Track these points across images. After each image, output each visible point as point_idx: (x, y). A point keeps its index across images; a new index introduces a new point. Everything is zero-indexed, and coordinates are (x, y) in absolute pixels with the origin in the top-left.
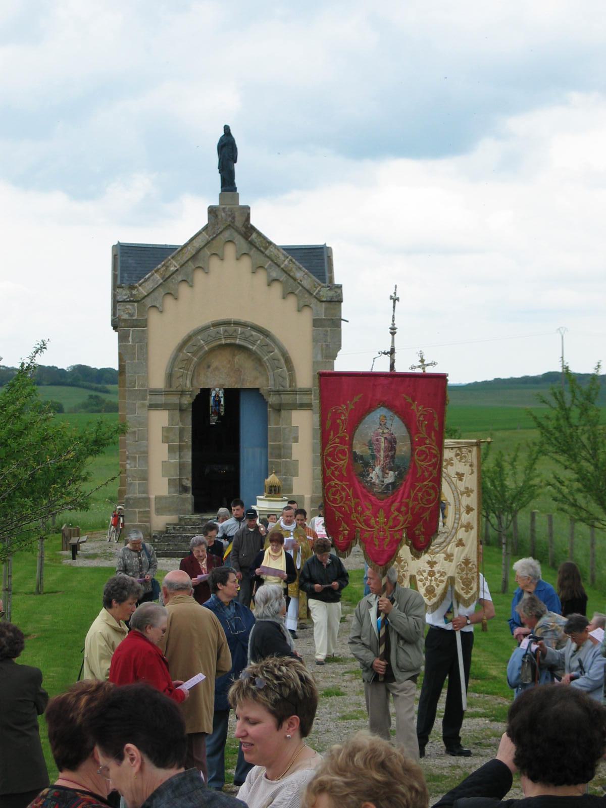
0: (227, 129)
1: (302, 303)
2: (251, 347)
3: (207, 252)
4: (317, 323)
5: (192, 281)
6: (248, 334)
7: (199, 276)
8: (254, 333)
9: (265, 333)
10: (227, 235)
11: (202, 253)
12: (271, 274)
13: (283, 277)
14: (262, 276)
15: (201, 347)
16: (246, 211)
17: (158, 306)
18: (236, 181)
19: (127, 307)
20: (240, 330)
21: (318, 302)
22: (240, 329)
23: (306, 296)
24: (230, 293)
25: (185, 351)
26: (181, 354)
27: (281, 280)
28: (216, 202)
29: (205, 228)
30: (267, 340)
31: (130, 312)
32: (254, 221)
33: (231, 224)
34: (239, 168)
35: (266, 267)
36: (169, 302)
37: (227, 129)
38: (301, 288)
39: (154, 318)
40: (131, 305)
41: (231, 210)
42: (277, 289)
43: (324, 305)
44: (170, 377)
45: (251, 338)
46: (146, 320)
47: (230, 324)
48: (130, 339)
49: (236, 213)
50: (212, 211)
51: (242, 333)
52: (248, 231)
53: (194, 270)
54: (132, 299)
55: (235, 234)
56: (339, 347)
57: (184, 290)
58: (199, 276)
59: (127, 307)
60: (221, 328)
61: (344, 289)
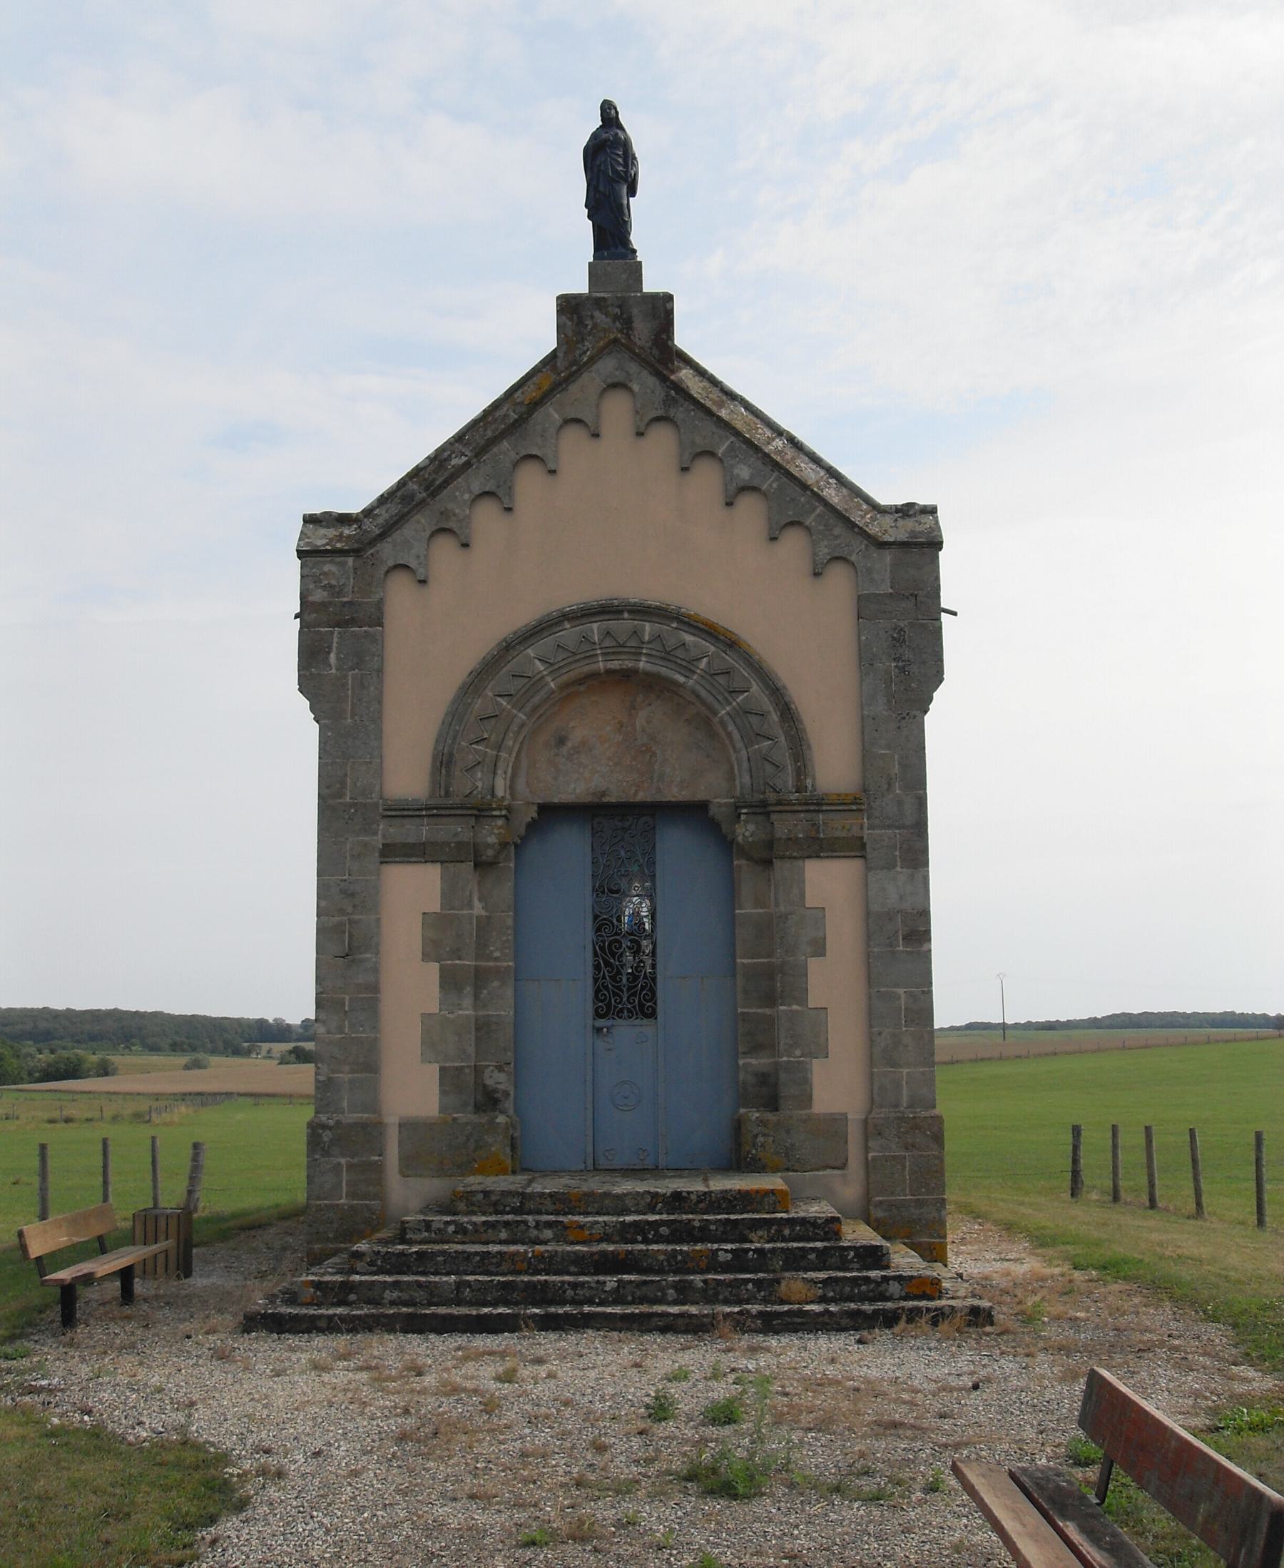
0: (609, 114)
1: (824, 551)
2: (682, 679)
3: (552, 413)
4: (866, 607)
5: (510, 490)
6: (671, 642)
7: (529, 482)
8: (689, 638)
9: (730, 643)
10: (608, 366)
11: (538, 416)
12: (736, 471)
13: (771, 482)
14: (707, 478)
15: (536, 683)
16: (662, 307)
17: (413, 564)
18: (636, 239)
19: (326, 568)
20: (648, 628)
21: (872, 548)
22: (648, 626)
23: (837, 531)
24: (616, 526)
25: (490, 694)
26: (479, 703)
27: (764, 487)
28: (580, 285)
29: (551, 359)
30: (730, 660)
31: (334, 582)
32: (683, 339)
33: (617, 334)
34: (640, 209)
35: (720, 452)
36: (444, 552)
37: (609, 114)
38: (820, 509)
39: (400, 599)
40: (332, 562)
41: (622, 304)
42: (751, 511)
43: (888, 557)
44: (443, 762)
45: (680, 653)
46: (380, 605)
47: (621, 612)
48: (332, 658)
49: (635, 311)
50: (568, 306)
51: (658, 638)
52: (662, 355)
53: (516, 465)
54: (339, 545)
55: (633, 367)
56: (936, 677)
57: (486, 518)
58: (529, 482)
59: (326, 568)
60: (595, 626)
61: (940, 514)
